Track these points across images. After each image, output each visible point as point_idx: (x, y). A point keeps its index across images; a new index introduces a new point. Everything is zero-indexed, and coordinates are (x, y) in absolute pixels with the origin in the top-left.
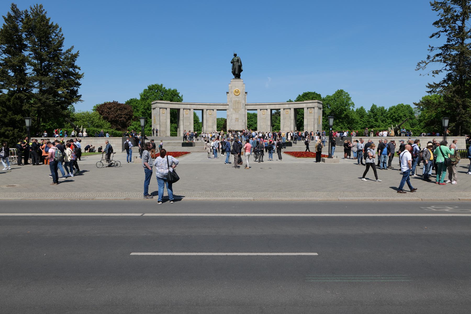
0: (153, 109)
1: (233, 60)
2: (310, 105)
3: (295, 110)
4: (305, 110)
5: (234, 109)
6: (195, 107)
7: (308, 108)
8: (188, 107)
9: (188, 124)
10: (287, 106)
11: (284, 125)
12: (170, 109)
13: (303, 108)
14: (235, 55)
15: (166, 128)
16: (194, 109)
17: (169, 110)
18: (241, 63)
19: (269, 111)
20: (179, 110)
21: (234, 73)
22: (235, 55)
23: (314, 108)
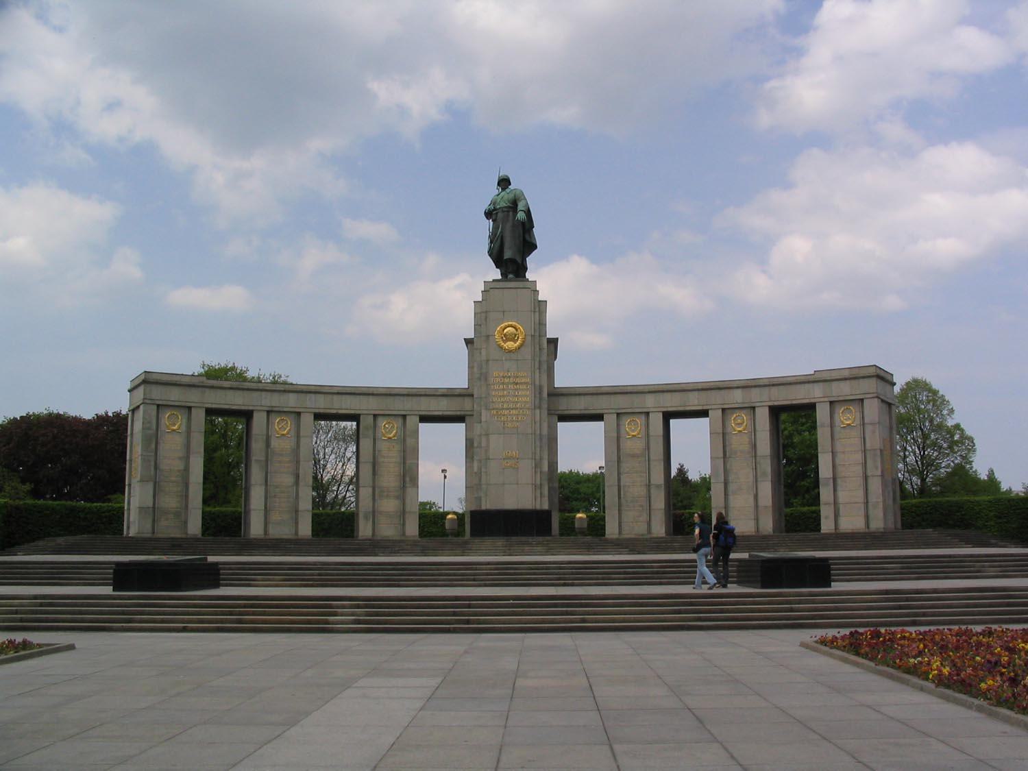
1: (494, 203)
2: (845, 390)
3: (776, 412)
4: (822, 414)
6: (321, 404)
7: (831, 403)
8: (291, 401)
9: (288, 480)
10: (737, 397)
11: (726, 484)
12: (210, 412)
13: (811, 407)
14: (504, 183)
15: (185, 497)
16: (318, 417)
17: (199, 417)
18: (528, 213)
19: (657, 421)
20: (247, 415)
21: (497, 257)
22: (504, 183)
23: (862, 400)
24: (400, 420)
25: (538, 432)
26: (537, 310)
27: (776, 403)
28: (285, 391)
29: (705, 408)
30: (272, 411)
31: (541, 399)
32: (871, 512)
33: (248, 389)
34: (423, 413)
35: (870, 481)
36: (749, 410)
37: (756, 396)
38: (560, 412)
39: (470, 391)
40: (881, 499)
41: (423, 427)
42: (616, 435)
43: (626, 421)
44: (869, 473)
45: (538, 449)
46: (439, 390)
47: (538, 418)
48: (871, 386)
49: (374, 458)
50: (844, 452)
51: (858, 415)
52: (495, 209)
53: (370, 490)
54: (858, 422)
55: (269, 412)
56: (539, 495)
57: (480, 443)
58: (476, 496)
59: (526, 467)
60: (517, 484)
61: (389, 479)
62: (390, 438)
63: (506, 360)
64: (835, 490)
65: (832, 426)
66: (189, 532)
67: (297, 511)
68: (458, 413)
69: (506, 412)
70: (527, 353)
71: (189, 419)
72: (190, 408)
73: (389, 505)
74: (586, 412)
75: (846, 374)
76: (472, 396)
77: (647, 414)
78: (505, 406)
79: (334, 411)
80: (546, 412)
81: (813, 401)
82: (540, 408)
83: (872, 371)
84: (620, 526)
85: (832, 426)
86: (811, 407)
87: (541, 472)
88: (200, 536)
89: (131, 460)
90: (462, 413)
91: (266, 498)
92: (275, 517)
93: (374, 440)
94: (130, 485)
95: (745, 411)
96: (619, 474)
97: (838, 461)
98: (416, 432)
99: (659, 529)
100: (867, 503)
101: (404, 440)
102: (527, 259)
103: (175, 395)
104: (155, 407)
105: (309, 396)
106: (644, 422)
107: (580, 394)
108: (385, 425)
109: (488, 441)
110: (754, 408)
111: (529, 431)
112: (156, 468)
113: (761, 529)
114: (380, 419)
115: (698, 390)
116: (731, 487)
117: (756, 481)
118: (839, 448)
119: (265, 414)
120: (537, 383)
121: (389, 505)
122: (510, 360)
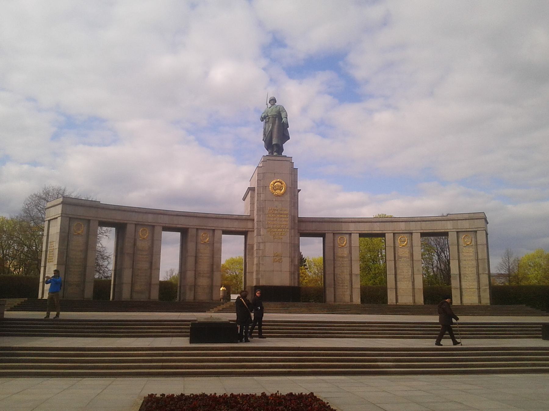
0: (49, 221)
2: (466, 225)
4: (452, 237)
6: (166, 221)
7: (457, 232)
8: (150, 219)
9: (146, 265)
10: (402, 227)
22: (273, 101)
24: (211, 232)
25: (293, 242)
27: (425, 231)
28: (146, 213)
29: (383, 232)
30: (138, 224)
31: (295, 223)
32: (482, 294)
33: (125, 211)
34: (224, 229)
35: (481, 276)
36: (409, 235)
37: (412, 226)
38: (300, 231)
40: (488, 287)
41: (224, 236)
42: (332, 245)
43: (338, 238)
44: (480, 272)
47: (293, 235)
48: (481, 223)
49: (196, 253)
50: (465, 260)
51: (473, 239)
52: (268, 116)
53: (193, 273)
54: (473, 243)
55: (136, 224)
57: (259, 247)
61: (204, 267)
62: (205, 242)
64: (460, 281)
65: (458, 245)
66: (86, 297)
67: (150, 284)
68: (244, 230)
69: (275, 230)
70: (287, 197)
71: (89, 226)
72: (89, 220)
73: (203, 282)
74: (316, 232)
75: (467, 216)
76: (254, 220)
77: (350, 234)
78: (274, 227)
79: (174, 226)
80: (297, 231)
81: (446, 231)
82: (294, 228)
83: (482, 215)
84: (335, 297)
85: (458, 245)
86: (446, 234)
88: (92, 299)
89: (46, 251)
90: (247, 230)
91: (132, 276)
92: (137, 288)
93: (197, 243)
94: (45, 267)
95: (407, 235)
96: (334, 267)
97: (461, 266)
98: (220, 239)
99: (357, 300)
100: (479, 289)
101: (213, 244)
103: (80, 212)
104: (68, 219)
105: (160, 216)
106: (348, 239)
107: (312, 222)
109: (265, 245)
110: (412, 233)
111: (288, 241)
112: (67, 256)
113: (416, 301)
114: (200, 231)
115: (380, 222)
116: (399, 277)
117: (413, 273)
118: (462, 258)
119: (133, 226)
121: (203, 282)
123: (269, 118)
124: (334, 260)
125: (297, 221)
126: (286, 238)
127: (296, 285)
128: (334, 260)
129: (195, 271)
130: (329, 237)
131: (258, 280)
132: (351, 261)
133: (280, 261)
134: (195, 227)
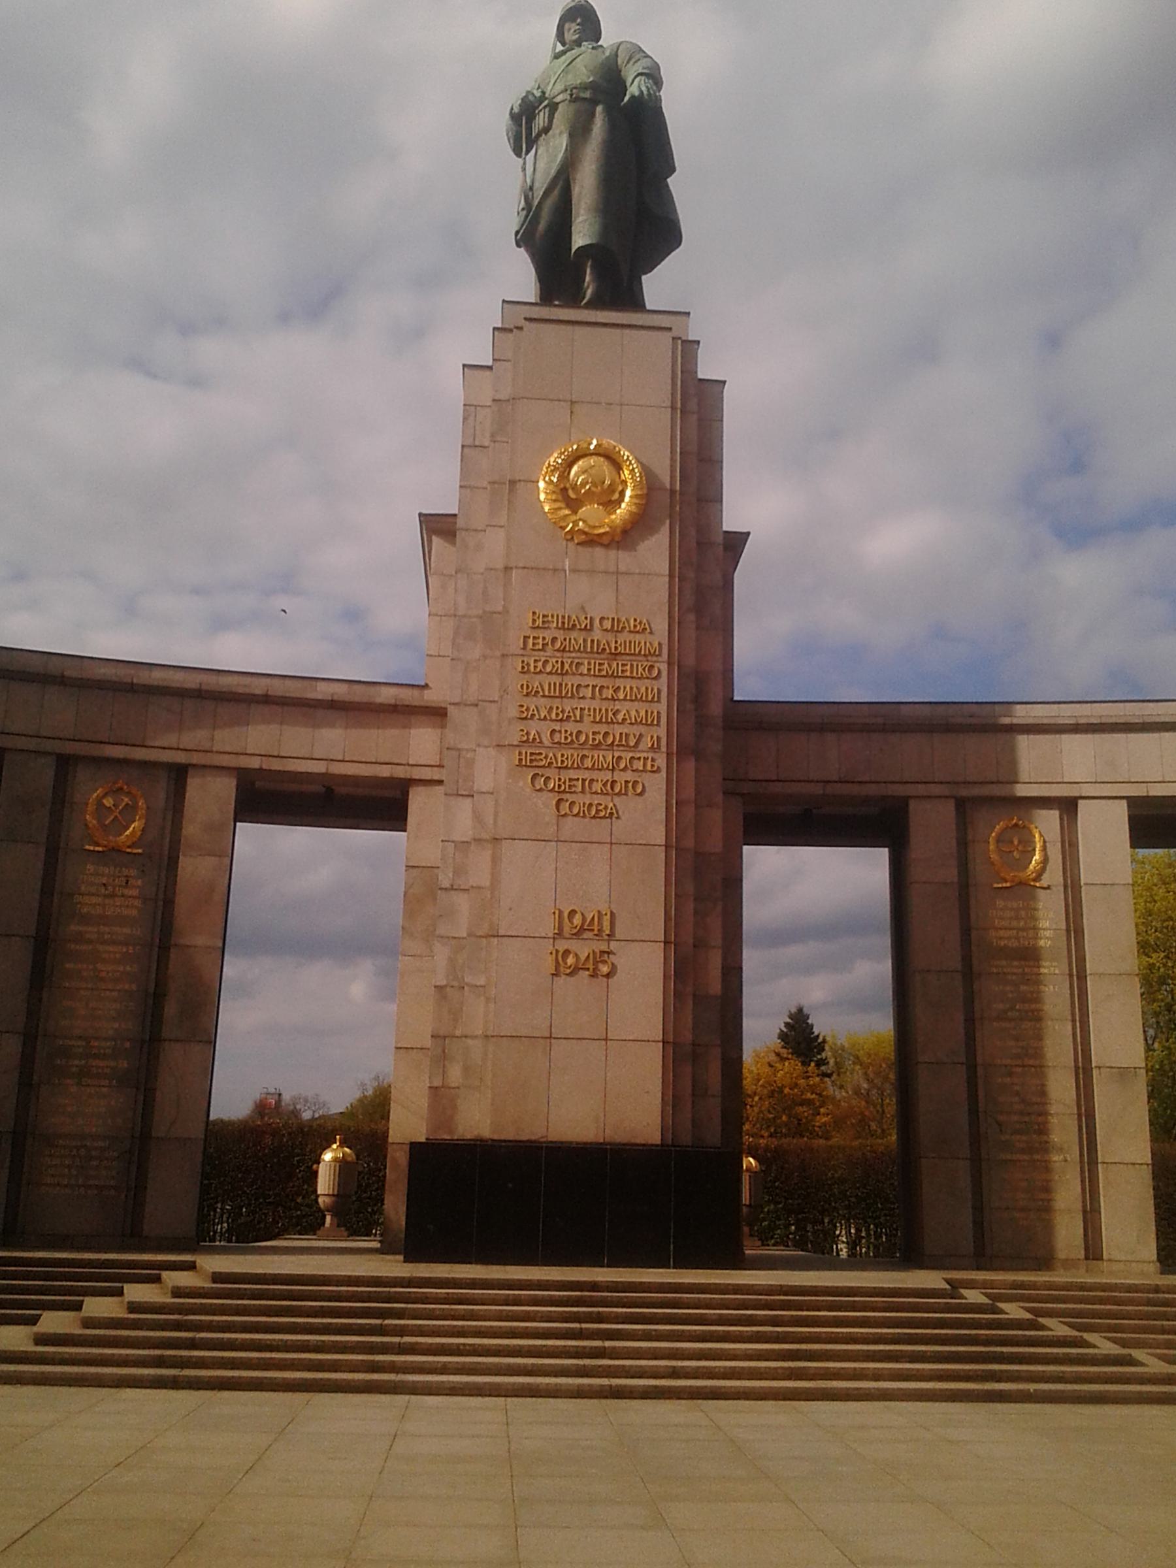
5: (531, 759)
25: (689, 843)
26: (693, 405)
31: (702, 722)
39: (431, 697)
42: (951, 874)
45: (690, 906)
46: (321, 686)
47: (689, 793)
56: (689, 1090)
58: (437, 1082)
59: (642, 971)
60: (606, 1040)
62: (117, 850)
63: (574, 571)
68: (385, 772)
87: (694, 995)
90: (401, 773)
96: (970, 1022)
102: (644, 278)
108: (99, 803)
120: (690, 661)
122: (592, 572)
123: (553, 107)
124: (969, 974)
125: (715, 709)
126: (646, 814)
127: (713, 1136)
128: (969, 974)
129: (30, 1037)
130: (931, 825)
131: (441, 1098)
132: (1082, 977)
133: (599, 967)
134: (49, 746)
